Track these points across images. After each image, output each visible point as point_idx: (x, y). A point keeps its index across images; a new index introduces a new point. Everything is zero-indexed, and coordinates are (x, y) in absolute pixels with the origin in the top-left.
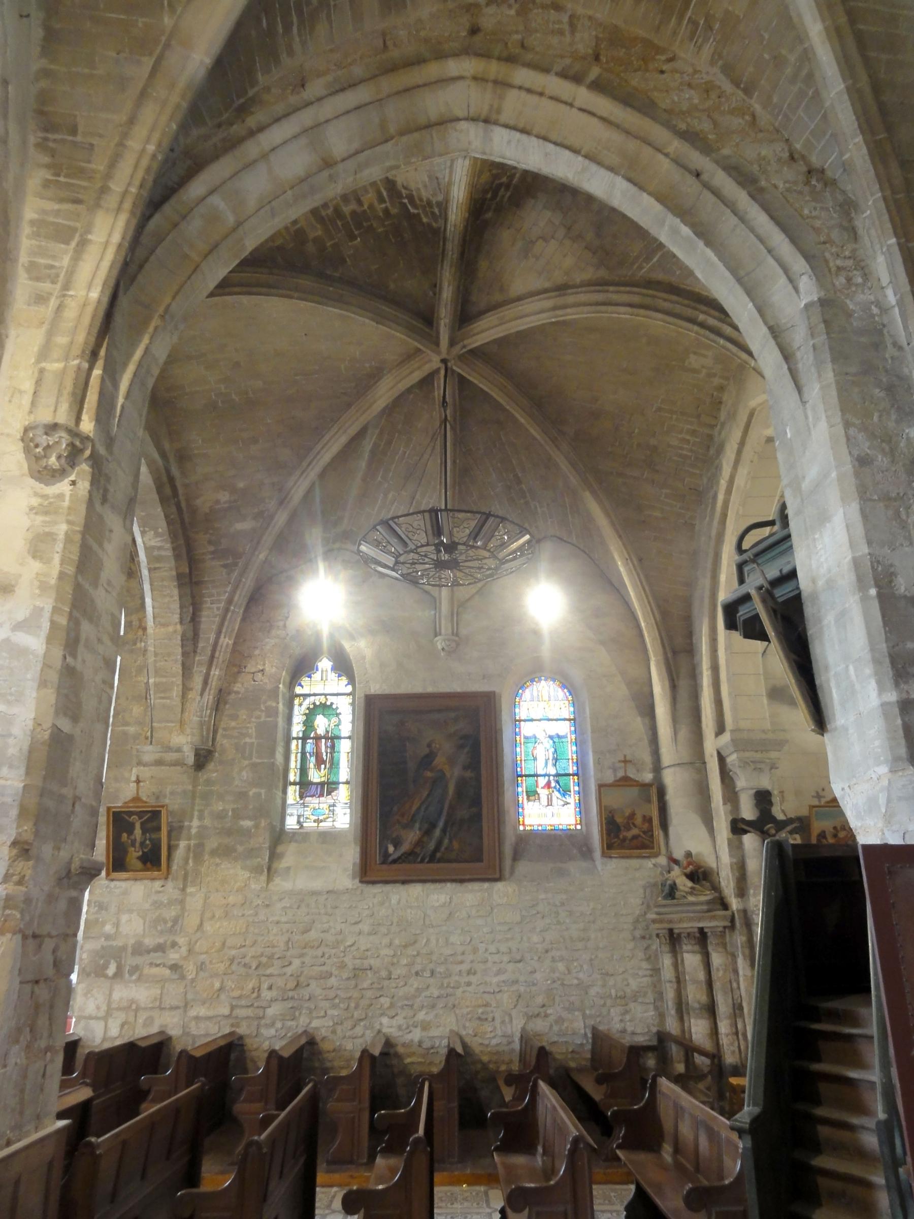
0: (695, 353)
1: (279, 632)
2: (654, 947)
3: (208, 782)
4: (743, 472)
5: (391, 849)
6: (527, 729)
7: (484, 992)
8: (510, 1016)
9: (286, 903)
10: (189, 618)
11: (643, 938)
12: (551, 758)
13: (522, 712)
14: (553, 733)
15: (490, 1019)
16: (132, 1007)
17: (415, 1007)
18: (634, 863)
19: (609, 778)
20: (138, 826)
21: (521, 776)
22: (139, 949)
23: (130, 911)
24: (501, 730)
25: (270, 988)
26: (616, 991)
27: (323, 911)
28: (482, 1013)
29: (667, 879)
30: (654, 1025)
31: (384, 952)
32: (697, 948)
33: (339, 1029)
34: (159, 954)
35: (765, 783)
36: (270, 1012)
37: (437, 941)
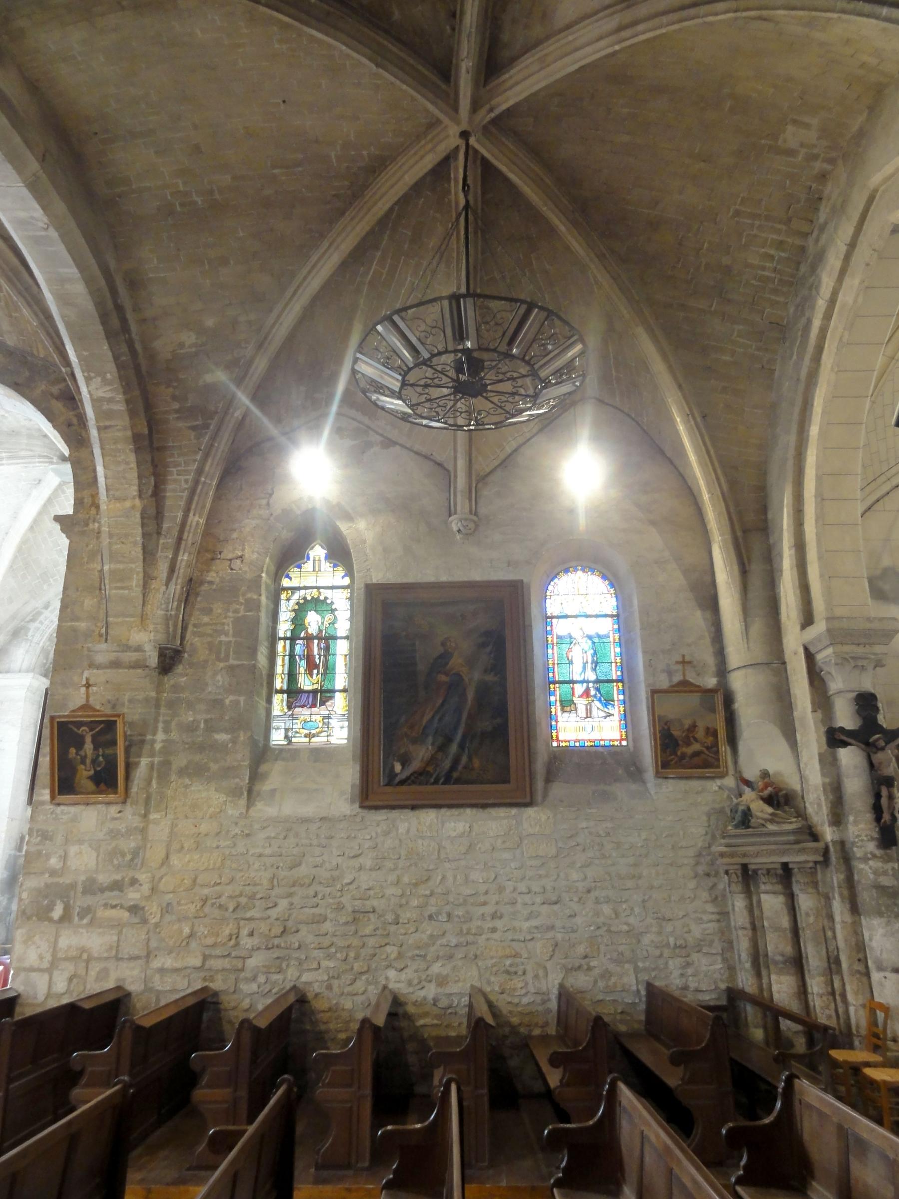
0: (795, 122)
1: (261, 512)
2: (721, 886)
3: (176, 688)
4: (852, 282)
5: (398, 768)
6: (560, 628)
7: (513, 940)
8: (545, 968)
9: (271, 832)
10: (150, 492)
11: (708, 875)
12: (590, 661)
13: (552, 607)
14: (592, 633)
15: (520, 973)
16: (83, 957)
17: (428, 958)
18: (695, 784)
19: (664, 682)
20: (88, 739)
21: (554, 683)
22: (91, 888)
23: (81, 842)
24: (531, 626)
25: (251, 934)
26: (676, 939)
27: (315, 842)
28: (511, 965)
29: (738, 804)
30: (722, 980)
31: (390, 891)
32: (779, 888)
33: (335, 983)
34: (116, 893)
35: (867, 685)
36: (251, 963)
37: (455, 877)
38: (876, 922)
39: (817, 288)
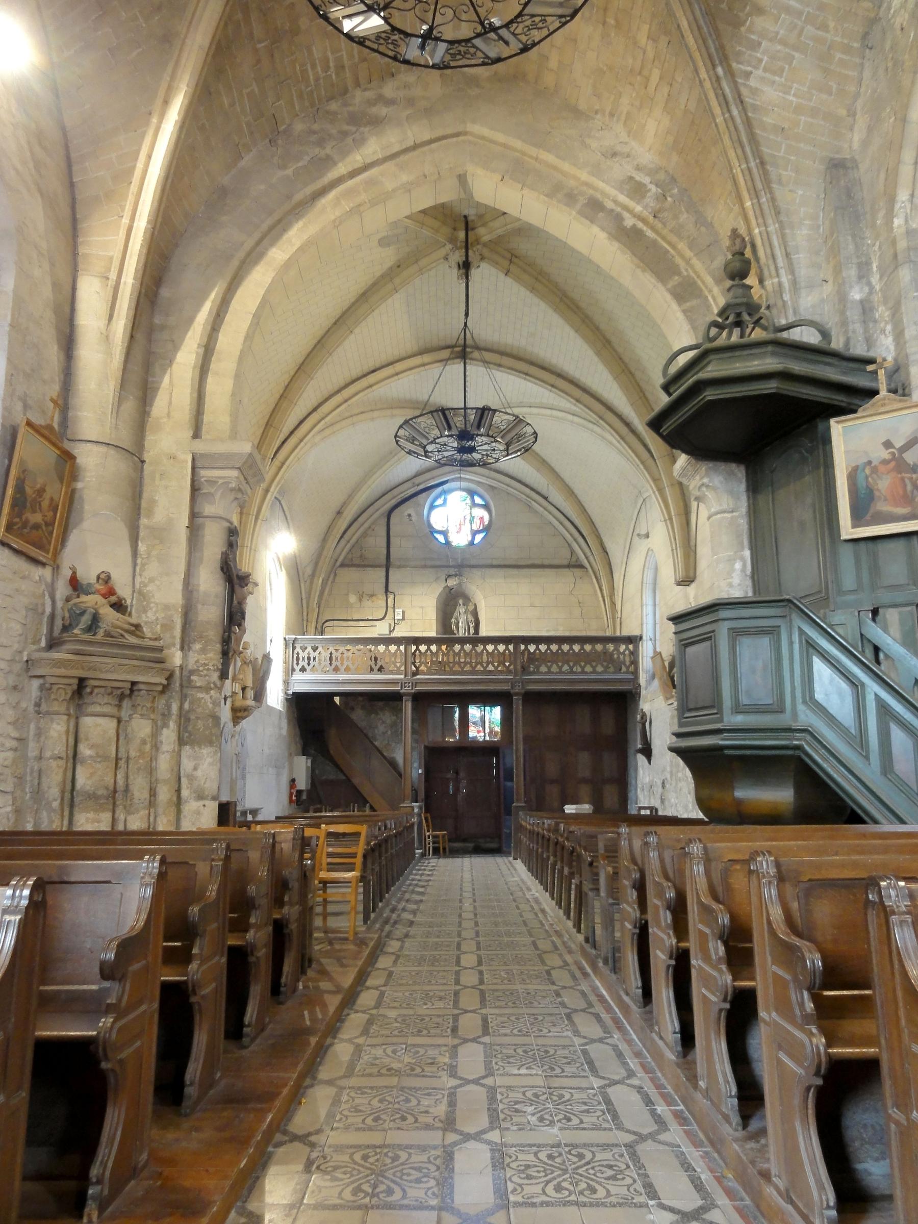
38: (206, 751)
39: (360, 142)
